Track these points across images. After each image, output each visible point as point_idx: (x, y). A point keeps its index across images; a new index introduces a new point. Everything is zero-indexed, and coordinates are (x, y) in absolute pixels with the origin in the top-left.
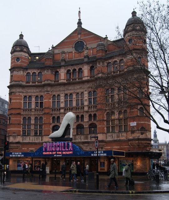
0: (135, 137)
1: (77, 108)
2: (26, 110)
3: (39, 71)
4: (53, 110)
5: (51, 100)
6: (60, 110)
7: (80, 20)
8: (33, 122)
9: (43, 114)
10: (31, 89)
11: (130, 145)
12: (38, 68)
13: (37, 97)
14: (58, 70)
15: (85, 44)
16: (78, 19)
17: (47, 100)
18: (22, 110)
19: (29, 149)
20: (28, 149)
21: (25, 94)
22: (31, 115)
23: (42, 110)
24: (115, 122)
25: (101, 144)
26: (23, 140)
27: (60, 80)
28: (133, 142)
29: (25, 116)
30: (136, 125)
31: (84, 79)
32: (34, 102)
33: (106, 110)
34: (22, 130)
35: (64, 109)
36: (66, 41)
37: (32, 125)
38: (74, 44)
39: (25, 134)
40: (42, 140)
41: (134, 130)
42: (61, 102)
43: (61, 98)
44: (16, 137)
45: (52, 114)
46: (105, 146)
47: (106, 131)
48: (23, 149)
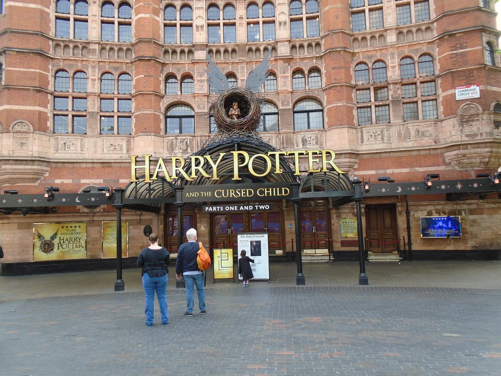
0: (476, 135)
1: (250, 50)
2: (66, 46)
4: (166, 52)
5: (160, 19)
6: (190, 52)
9: (132, 63)
11: (450, 164)
17: (148, 16)
18: (51, 43)
23: (128, 50)
24: (391, 93)
25: (347, 160)
28: (471, 151)
29: (62, 65)
30: (479, 96)
32: (96, 18)
33: (353, 54)
34: (50, 115)
35: (208, 49)
37: (89, 98)
41: (472, 112)
42: (197, 27)
43: (196, 13)
45: (164, 64)
46: (356, 166)
47: (355, 121)
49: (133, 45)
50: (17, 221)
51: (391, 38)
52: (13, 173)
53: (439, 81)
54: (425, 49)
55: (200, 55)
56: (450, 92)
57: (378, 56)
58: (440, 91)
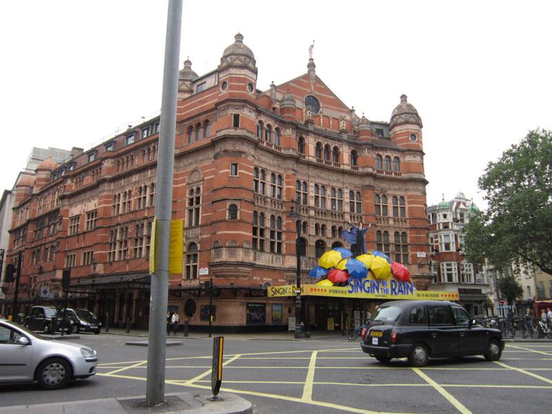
3: (276, 126)
7: (311, 59)
8: (268, 224)
10: (266, 156)
12: (276, 120)
13: (273, 175)
14: (304, 136)
15: (321, 106)
16: (309, 58)
19: (264, 279)
20: (262, 279)
21: (256, 163)
22: (266, 208)
26: (255, 259)
27: (309, 156)
28: (422, 280)
31: (342, 167)
36: (292, 84)
38: (305, 97)
39: (257, 245)
40: (283, 262)
41: (423, 263)
44: (248, 252)
48: (255, 278)
49: (284, 202)
50: (239, 300)
51: (391, 222)
52: (242, 272)
53: (409, 247)
54: (404, 230)
55: (312, 213)
56: (414, 253)
57: (386, 229)
58: (409, 251)
